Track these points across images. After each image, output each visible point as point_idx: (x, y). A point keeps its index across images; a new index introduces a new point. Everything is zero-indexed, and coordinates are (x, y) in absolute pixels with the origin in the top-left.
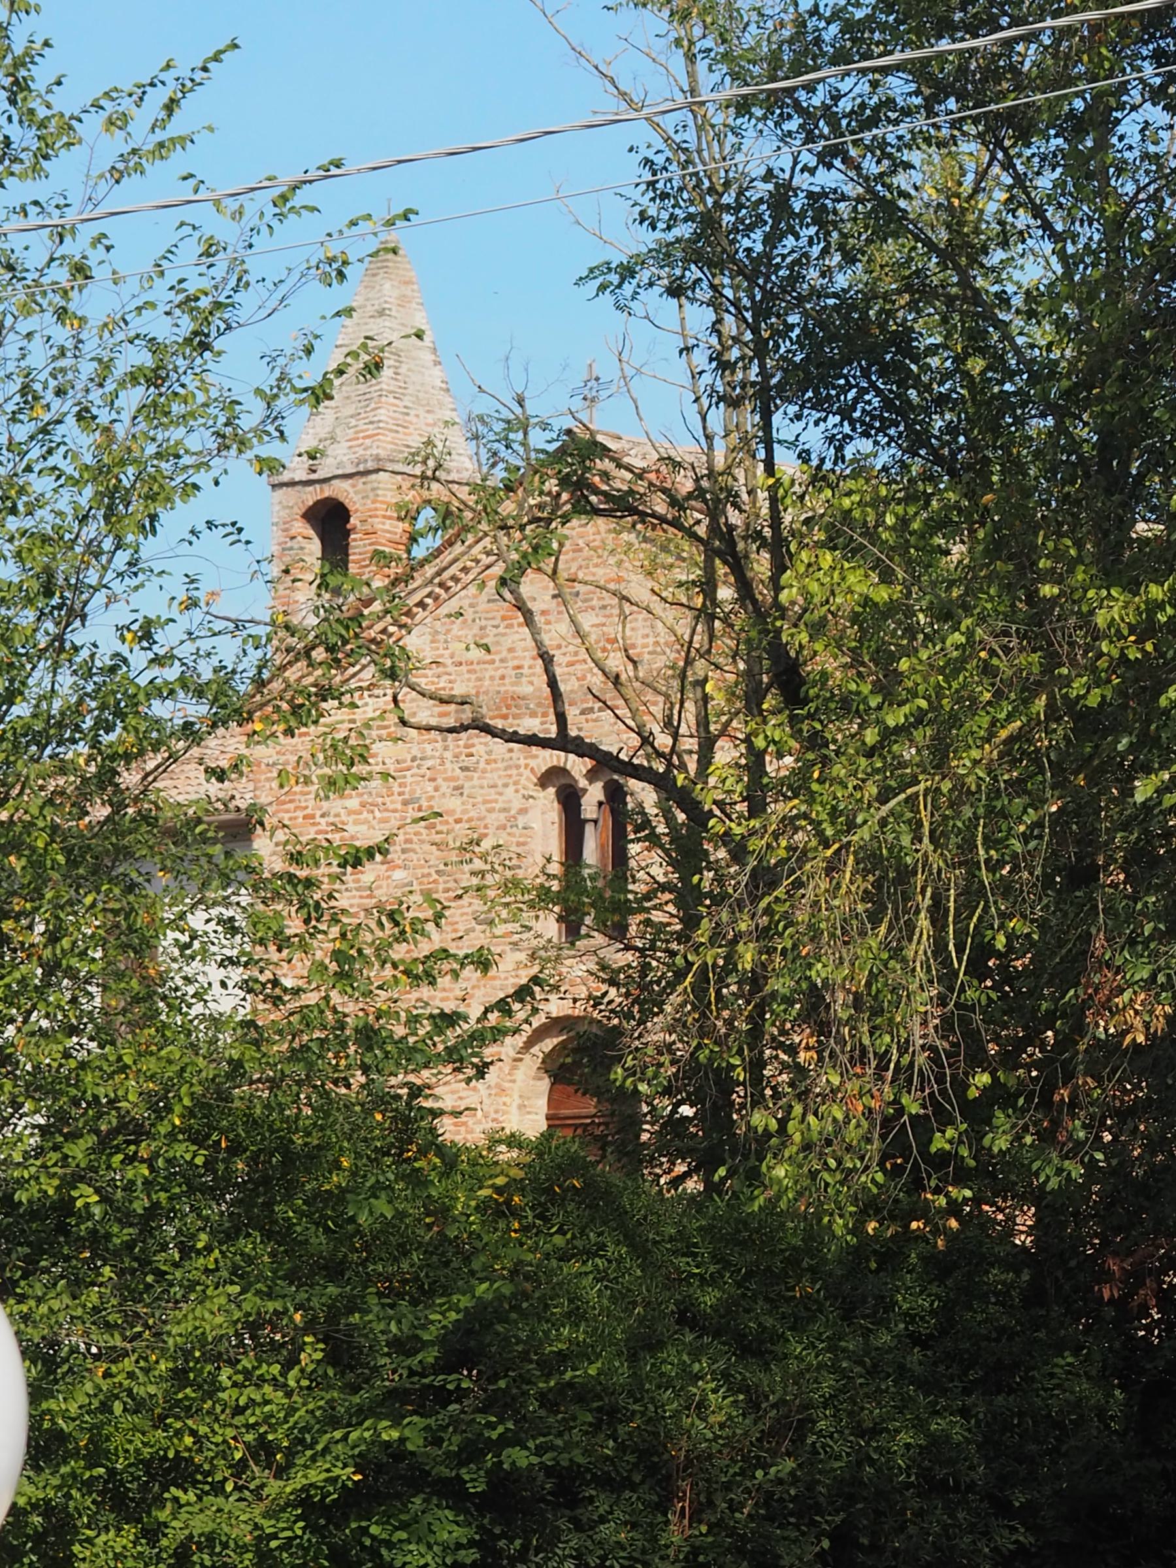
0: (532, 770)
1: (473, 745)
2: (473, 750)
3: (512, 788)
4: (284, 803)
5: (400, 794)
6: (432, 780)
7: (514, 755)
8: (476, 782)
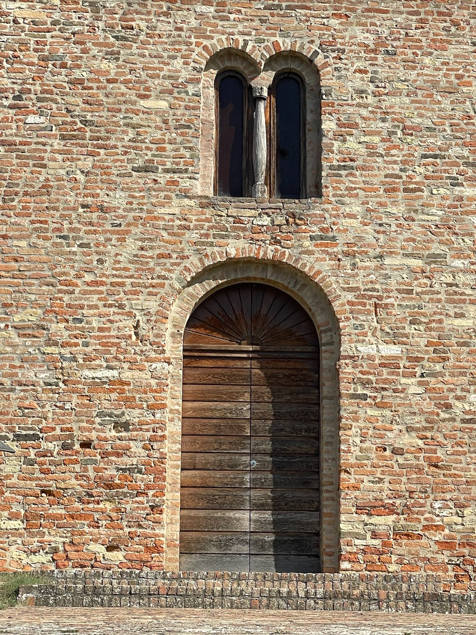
0: (205, 48)
2: (134, 24)
7: (183, 34)
8: (134, 50)
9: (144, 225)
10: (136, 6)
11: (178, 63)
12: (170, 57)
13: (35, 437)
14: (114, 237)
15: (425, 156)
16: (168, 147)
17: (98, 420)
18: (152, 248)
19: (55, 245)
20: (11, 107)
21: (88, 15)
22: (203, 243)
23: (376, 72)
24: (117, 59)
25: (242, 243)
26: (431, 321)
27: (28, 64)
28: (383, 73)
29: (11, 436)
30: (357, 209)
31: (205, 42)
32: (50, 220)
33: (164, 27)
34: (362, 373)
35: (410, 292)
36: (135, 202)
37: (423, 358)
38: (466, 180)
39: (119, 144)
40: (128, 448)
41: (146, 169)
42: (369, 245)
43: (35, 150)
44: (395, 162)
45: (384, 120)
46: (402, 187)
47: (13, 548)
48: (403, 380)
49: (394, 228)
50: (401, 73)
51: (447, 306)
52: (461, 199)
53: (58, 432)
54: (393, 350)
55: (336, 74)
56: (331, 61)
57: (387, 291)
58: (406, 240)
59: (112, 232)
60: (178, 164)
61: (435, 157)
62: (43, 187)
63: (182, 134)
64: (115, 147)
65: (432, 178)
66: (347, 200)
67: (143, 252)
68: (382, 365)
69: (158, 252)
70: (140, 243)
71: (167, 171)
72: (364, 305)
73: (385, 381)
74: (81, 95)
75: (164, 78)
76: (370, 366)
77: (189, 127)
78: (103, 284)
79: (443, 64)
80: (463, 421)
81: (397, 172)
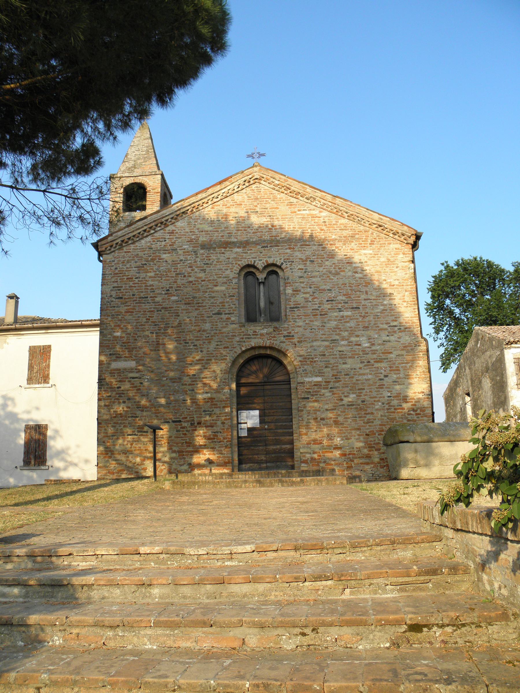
0: (239, 265)
1: (210, 257)
3: (229, 270)
4: (118, 274)
5: (174, 272)
6: (191, 267)
8: (211, 268)
9: (218, 336)
10: (212, 251)
11: (228, 272)
12: (225, 269)
13: (180, 421)
14: (206, 341)
15: (327, 301)
16: (226, 304)
17: (203, 413)
18: (221, 345)
19: (184, 346)
20: (166, 294)
21: (193, 256)
22: (241, 342)
23: (307, 269)
24: (205, 272)
25: (256, 340)
26: (333, 366)
27: (171, 277)
28: (309, 269)
29: (170, 421)
30: (301, 324)
31: (239, 263)
32: (181, 336)
33: (222, 258)
34: (306, 389)
35: (325, 355)
36: (214, 327)
37: (331, 382)
38: (345, 309)
39: (207, 305)
40: (216, 423)
41: (219, 313)
42: (307, 338)
43: (175, 310)
44: (316, 304)
45: (310, 288)
46: (319, 314)
47: (174, 464)
48: (323, 391)
49: (317, 330)
50: (317, 269)
51: (340, 360)
52: (343, 317)
53: (188, 419)
54: (319, 379)
55: (291, 271)
56: (288, 266)
57: (315, 355)
58: (323, 335)
59: (206, 339)
60: (230, 311)
61: (332, 301)
62: (179, 324)
63: (231, 299)
64: (205, 306)
65: (331, 309)
66: (297, 320)
67: (218, 347)
68: (315, 385)
69: (223, 346)
70: (216, 343)
71: (226, 314)
72: (306, 362)
73: (315, 392)
74: (192, 287)
75: (224, 277)
76: (310, 386)
77: (234, 296)
78: (203, 360)
79: (333, 264)
80: (348, 405)
81: (317, 308)
